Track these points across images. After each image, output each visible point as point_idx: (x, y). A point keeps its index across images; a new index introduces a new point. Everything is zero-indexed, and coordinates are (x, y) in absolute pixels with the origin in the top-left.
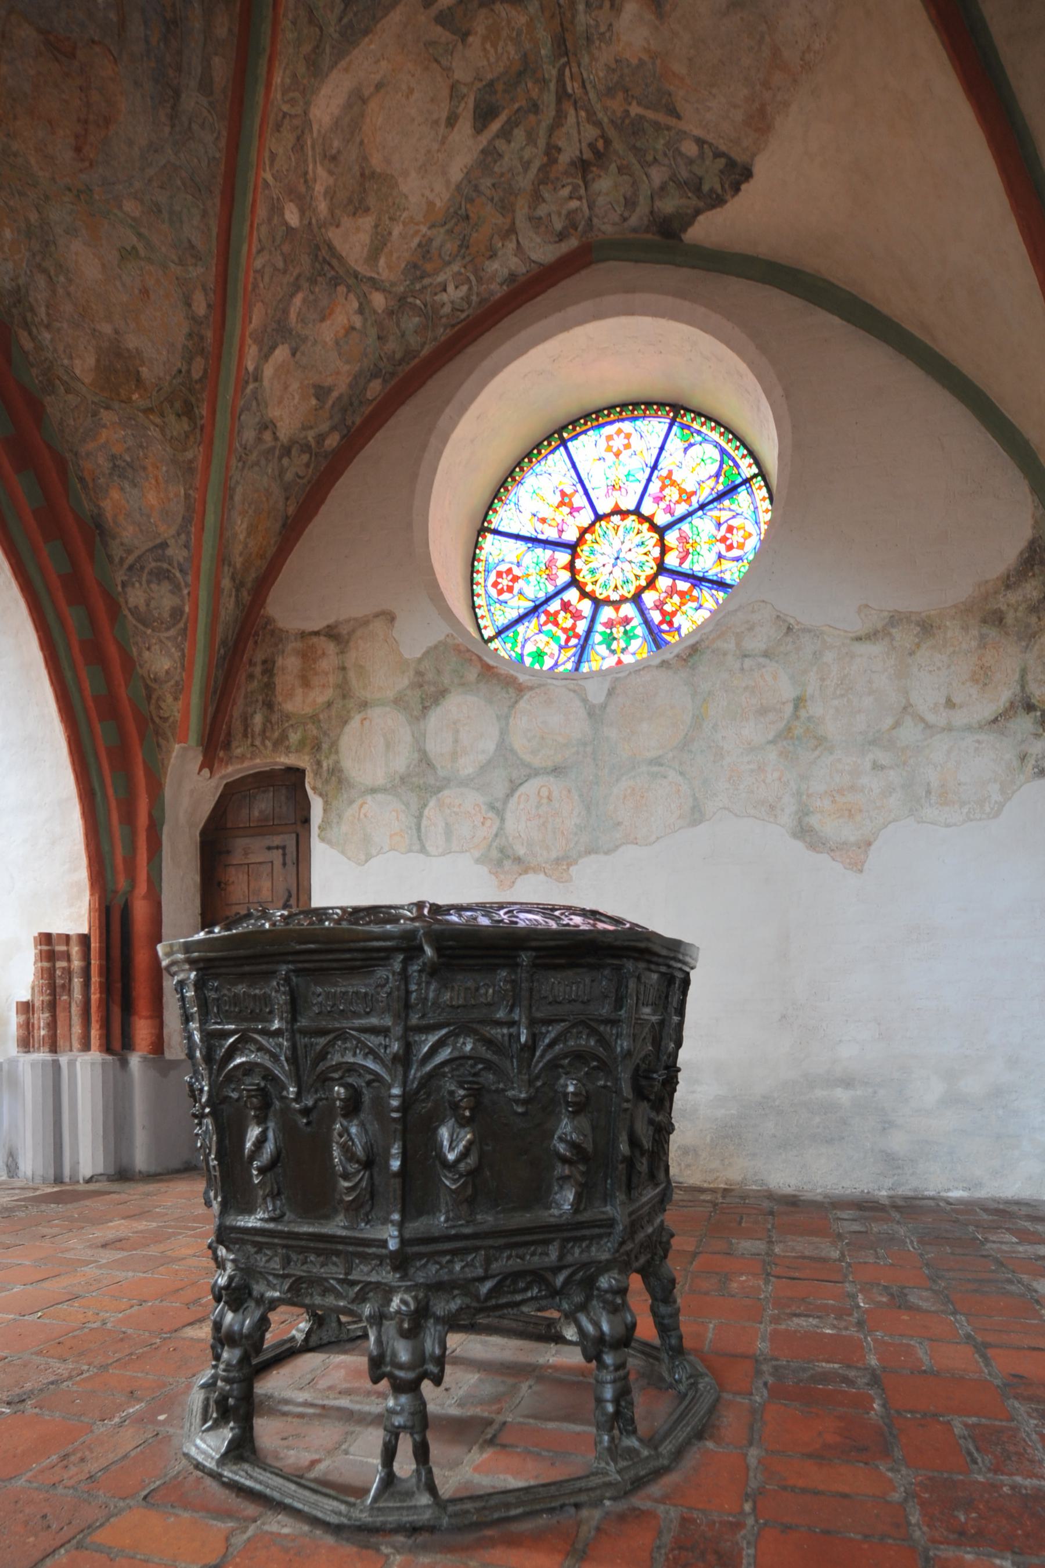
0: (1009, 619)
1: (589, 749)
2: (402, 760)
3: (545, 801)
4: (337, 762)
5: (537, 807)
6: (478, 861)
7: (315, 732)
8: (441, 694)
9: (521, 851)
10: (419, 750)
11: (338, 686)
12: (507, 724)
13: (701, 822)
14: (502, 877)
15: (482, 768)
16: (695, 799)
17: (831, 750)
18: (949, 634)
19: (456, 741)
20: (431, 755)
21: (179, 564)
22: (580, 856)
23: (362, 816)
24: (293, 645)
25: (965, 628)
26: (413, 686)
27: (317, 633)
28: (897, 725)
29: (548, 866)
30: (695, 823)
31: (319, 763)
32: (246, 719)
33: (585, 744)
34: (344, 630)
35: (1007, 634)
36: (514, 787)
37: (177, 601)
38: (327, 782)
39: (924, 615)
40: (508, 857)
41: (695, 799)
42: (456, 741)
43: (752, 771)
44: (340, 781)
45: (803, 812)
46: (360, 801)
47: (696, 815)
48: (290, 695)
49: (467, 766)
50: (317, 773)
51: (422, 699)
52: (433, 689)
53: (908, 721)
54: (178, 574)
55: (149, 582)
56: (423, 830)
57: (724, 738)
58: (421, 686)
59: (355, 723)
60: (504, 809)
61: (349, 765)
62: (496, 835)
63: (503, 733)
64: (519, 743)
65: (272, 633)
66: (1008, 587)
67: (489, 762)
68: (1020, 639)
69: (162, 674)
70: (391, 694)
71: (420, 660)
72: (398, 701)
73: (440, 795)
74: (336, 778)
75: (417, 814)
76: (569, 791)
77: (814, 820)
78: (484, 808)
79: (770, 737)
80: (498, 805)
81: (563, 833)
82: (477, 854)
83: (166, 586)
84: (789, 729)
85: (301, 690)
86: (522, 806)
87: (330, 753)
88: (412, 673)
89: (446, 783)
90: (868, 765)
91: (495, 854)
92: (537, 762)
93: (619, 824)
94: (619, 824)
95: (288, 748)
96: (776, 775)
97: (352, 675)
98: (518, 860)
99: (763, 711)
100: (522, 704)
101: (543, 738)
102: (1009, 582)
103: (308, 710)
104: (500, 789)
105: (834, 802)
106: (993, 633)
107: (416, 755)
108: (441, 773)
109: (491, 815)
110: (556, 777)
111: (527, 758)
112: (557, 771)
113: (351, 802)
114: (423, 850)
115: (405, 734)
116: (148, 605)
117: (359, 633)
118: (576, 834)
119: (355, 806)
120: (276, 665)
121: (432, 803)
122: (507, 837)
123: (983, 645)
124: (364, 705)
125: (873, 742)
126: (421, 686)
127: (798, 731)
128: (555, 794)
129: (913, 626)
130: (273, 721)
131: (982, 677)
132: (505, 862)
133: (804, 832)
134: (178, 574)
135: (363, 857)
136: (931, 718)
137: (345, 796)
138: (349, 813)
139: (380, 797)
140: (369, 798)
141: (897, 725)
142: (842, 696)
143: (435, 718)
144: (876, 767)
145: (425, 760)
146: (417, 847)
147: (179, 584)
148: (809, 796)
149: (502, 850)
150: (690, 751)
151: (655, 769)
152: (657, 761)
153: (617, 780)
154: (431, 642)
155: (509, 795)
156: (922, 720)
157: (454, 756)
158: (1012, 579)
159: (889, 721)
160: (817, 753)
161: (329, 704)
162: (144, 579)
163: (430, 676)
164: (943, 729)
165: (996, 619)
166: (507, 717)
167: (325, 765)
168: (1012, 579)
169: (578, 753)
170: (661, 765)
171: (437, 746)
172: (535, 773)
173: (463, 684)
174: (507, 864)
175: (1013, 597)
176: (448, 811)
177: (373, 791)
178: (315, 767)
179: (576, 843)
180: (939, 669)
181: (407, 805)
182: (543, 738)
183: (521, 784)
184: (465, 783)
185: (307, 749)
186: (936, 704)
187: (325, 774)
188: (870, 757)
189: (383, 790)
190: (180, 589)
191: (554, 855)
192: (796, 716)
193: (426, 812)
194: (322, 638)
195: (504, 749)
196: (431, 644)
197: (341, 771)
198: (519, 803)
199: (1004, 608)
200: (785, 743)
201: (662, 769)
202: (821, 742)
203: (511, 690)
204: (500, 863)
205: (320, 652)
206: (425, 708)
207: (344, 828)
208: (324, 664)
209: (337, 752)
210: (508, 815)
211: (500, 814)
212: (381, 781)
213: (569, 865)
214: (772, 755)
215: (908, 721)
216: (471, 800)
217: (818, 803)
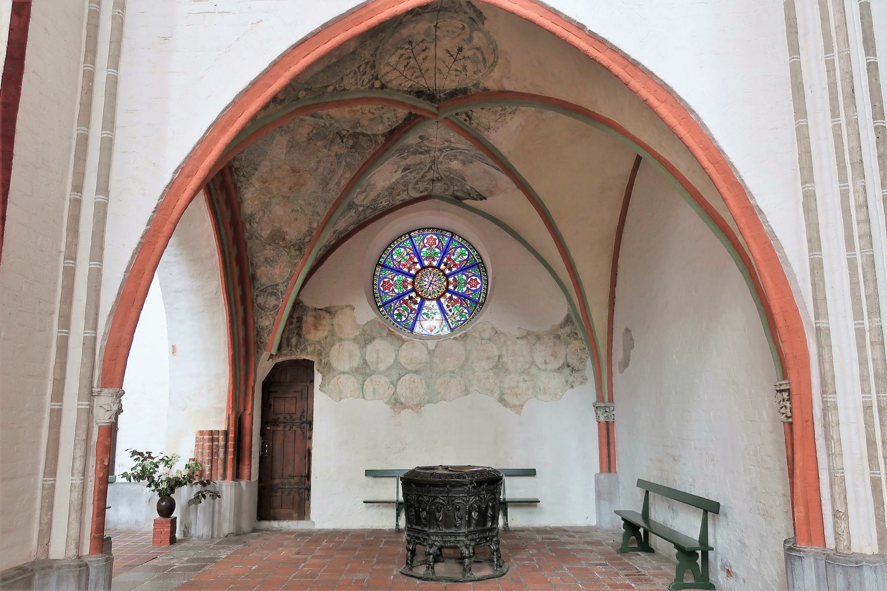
0: (562, 338)
1: (429, 365)
2: (356, 362)
3: (412, 383)
4: (329, 361)
5: (409, 385)
6: (386, 403)
7: (319, 348)
8: (372, 339)
9: (403, 401)
10: (363, 359)
11: (329, 331)
12: (398, 353)
13: (468, 394)
14: (395, 410)
15: (388, 368)
16: (466, 386)
17: (510, 373)
18: (545, 340)
19: (378, 357)
20: (368, 362)
21: (281, 291)
22: (425, 404)
23: (339, 383)
24: (311, 313)
25: (549, 339)
26: (361, 335)
27: (321, 310)
28: (530, 368)
29: (413, 407)
30: (466, 395)
31: (321, 360)
32: (288, 340)
33: (427, 363)
34: (333, 310)
35: (561, 342)
36: (400, 377)
37: (277, 303)
38: (324, 368)
39: (537, 333)
40: (398, 403)
41: (466, 386)
42: (378, 357)
43: (485, 378)
44: (329, 368)
45: (502, 394)
46: (338, 376)
47: (466, 392)
48: (309, 332)
49: (382, 367)
50: (320, 364)
51: (365, 340)
52: (369, 337)
53: (533, 367)
54: (280, 294)
55: (267, 296)
56: (364, 390)
57: (476, 366)
58: (364, 335)
59: (337, 346)
60: (396, 385)
61: (333, 362)
62: (393, 394)
63: (396, 356)
64: (403, 361)
65: (302, 307)
66: (561, 328)
67: (391, 366)
68: (565, 345)
69: (265, 327)
70: (352, 337)
71: (364, 325)
72: (355, 340)
73: (372, 377)
74: (328, 368)
75: (362, 383)
76: (421, 380)
77: (505, 397)
78: (389, 383)
79: (491, 368)
80: (395, 383)
81: (419, 395)
82: (386, 401)
83: (274, 298)
84: (497, 365)
85: (314, 331)
86: (403, 384)
87: (326, 357)
88: (361, 330)
89: (374, 373)
90: (522, 380)
91: (393, 401)
92: (410, 368)
93: (440, 393)
94: (440, 393)
95: (307, 353)
96: (493, 380)
97: (336, 327)
98: (402, 404)
99: (488, 358)
100: (404, 346)
101: (411, 360)
102: (562, 326)
103: (317, 339)
104: (395, 377)
105: (511, 391)
106: (557, 341)
107: (362, 361)
108: (372, 369)
109: (391, 386)
110: (416, 374)
111: (406, 366)
112: (416, 372)
113: (334, 377)
114: (364, 397)
115: (357, 352)
116: (265, 303)
117: (339, 312)
118: (423, 395)
119: (336, 378)
120: (303, 320)
121: (368, 380)
122: (398, 395)
123: (555, 345)
124: (341, 340)
125: (523, 372)
126: (364, 335)
127: (500, 366)
128: (416, 381)
129: (534, 336)
130: (301, 341)
131: (555, 355)
132: (397, 404)
133: (502, 400)
134: (280, 294)
135: (339, 399)
136: (540, 366)
137: (332, 374)
138: (333, 381)
139: (346, 376)
140: (342, 376)
141: (530, 368)
142: (513, 356)
143: (369, 348)
144: (524, 380)
145: (365, 362)
146: (362, 396)
147: (280, 297)
148: (503, 388)
149: (395, 400)
150: (464, 370)
151: (452, 375)
152: (453, 372)
153: (439, 377)
154: (369, 319)
155: (399, 379)
156: (538, 367)
157: (377, 363)
158: (563, 326)
159: (528, 366)
160: (506, 374)
161: (326, 338)
162: (266, 294)
163: (368, 332)
164: (544, 370)
165: (558, 337)
166: (398, 350)
167: (323, 361)
168: (563, 326)
169: (424, 366)
170: (454, 373)
171: (370, 358)
172: (409, 372)
173: (381, 337)
174: (398, 405)
175: (563, 331)
176: (374, 383)
177: (344, 373)
178: (319, 362)
179: (424, 399)
180: (542, 351)
181: (358, 380)
182: (411, 360)
183: (403, 376)
184: (381, 373)
185: (316, 354)
186: (542, 362)
187: (323, 365)
188: (522, 377)
189: (348, 373)
190: (279, 299)
191: (415, 403)
192: (499, 361)
193: (366, 383)
194: (324, 312)
195: (397, 362)
196: (369, 320)
197: (330, 364)
198: (402, 383)
199: (560, 334)
200: (495, 370)
201: (454, 375)
202: (507, 371)
203: (400, 341)
204: (395, 405)
205: (322, 317)
206: (366, 343)
207: (331, 387)
208: (324, 322)
209: (329, 357)
210: (399, 387)
211: (395, 386)
212: (347, 369)
213: (421, 407)
214: (491, 374)
215: (533, 367)
216: (384, 380)
217: (506, 391)
